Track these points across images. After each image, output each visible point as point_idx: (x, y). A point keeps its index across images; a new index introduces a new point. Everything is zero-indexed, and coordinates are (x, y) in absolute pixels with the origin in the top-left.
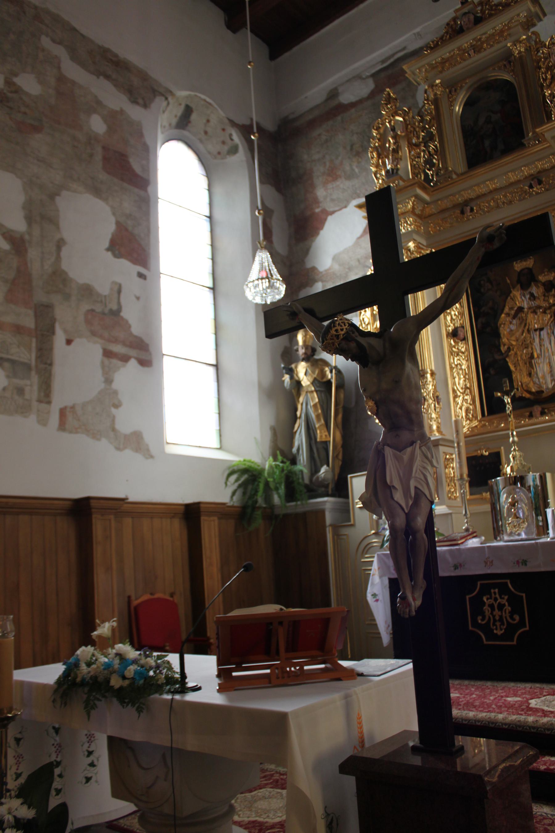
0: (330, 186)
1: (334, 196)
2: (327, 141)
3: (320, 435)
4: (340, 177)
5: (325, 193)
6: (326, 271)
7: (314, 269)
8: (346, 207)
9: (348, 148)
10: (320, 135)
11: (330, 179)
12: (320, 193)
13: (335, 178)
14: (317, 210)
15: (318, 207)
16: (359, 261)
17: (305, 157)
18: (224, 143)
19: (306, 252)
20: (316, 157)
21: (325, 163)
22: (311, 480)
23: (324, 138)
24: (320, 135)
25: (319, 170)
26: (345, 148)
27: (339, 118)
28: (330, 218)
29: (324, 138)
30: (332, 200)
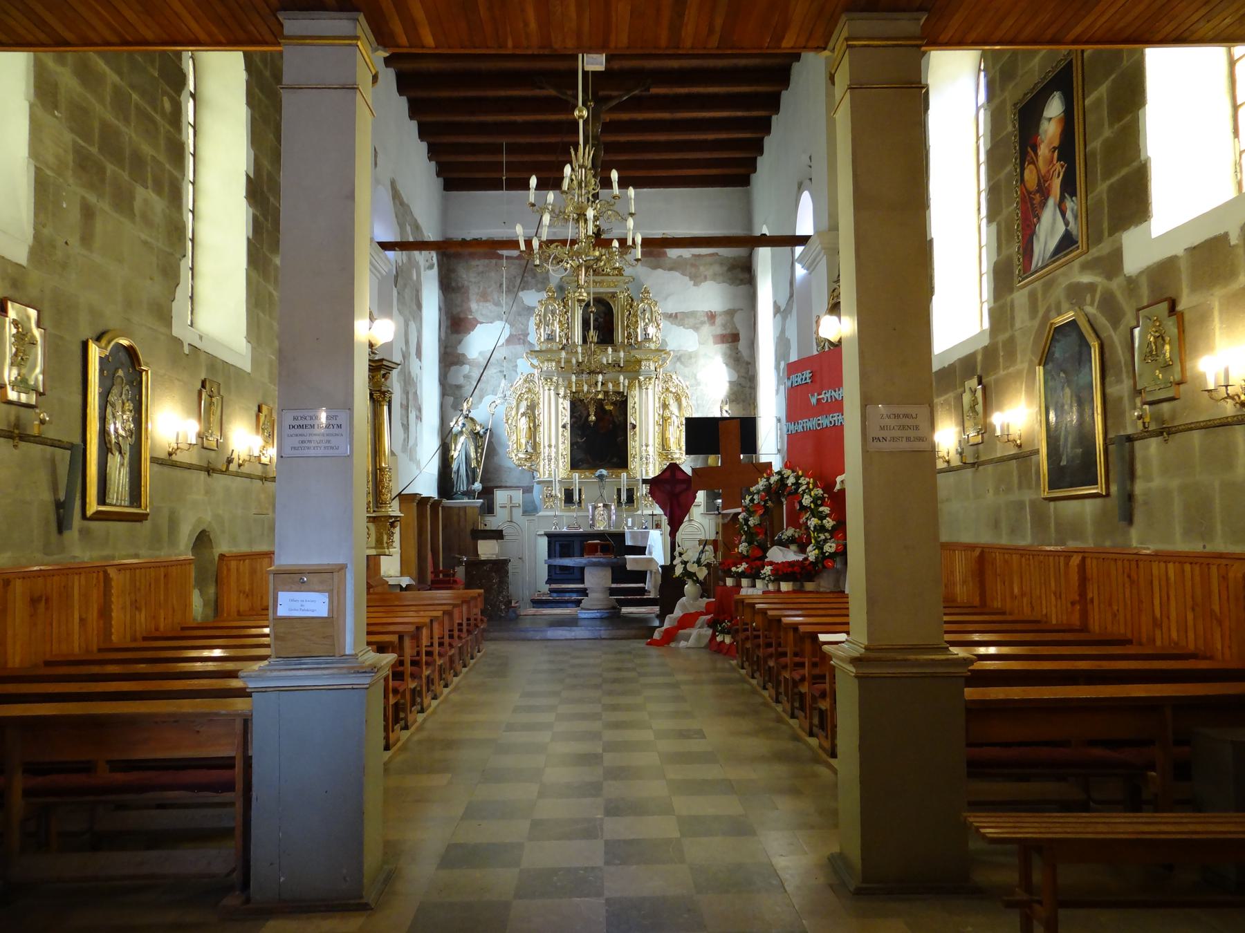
0: (481, 304)
1: (484, 312)
2: (482, 272)
3: (474, 464)
4: (490, 301)
5: (476, 307)
6: (473, 359)
7: (463, 355)
8: (491, 323)
9: (499, 285)
10: (477, 266)
11: (482, 299)
12: (474, 306)
13: (487, 301)
14: (470, 317)
15: (471, 315)
16: (497, 360)
17: (464, 276)
18: (427, 261)
19: (460, 342)
20: (473, 280)
21: (479, 287)
22: (467, 489)
23: (481, 269)
24: (477, 266)
25: (473, 292)
26: (496, 283)
27: (494, 261)
28: (479, 325)
29: (481, 269)
30: (482, 315)
